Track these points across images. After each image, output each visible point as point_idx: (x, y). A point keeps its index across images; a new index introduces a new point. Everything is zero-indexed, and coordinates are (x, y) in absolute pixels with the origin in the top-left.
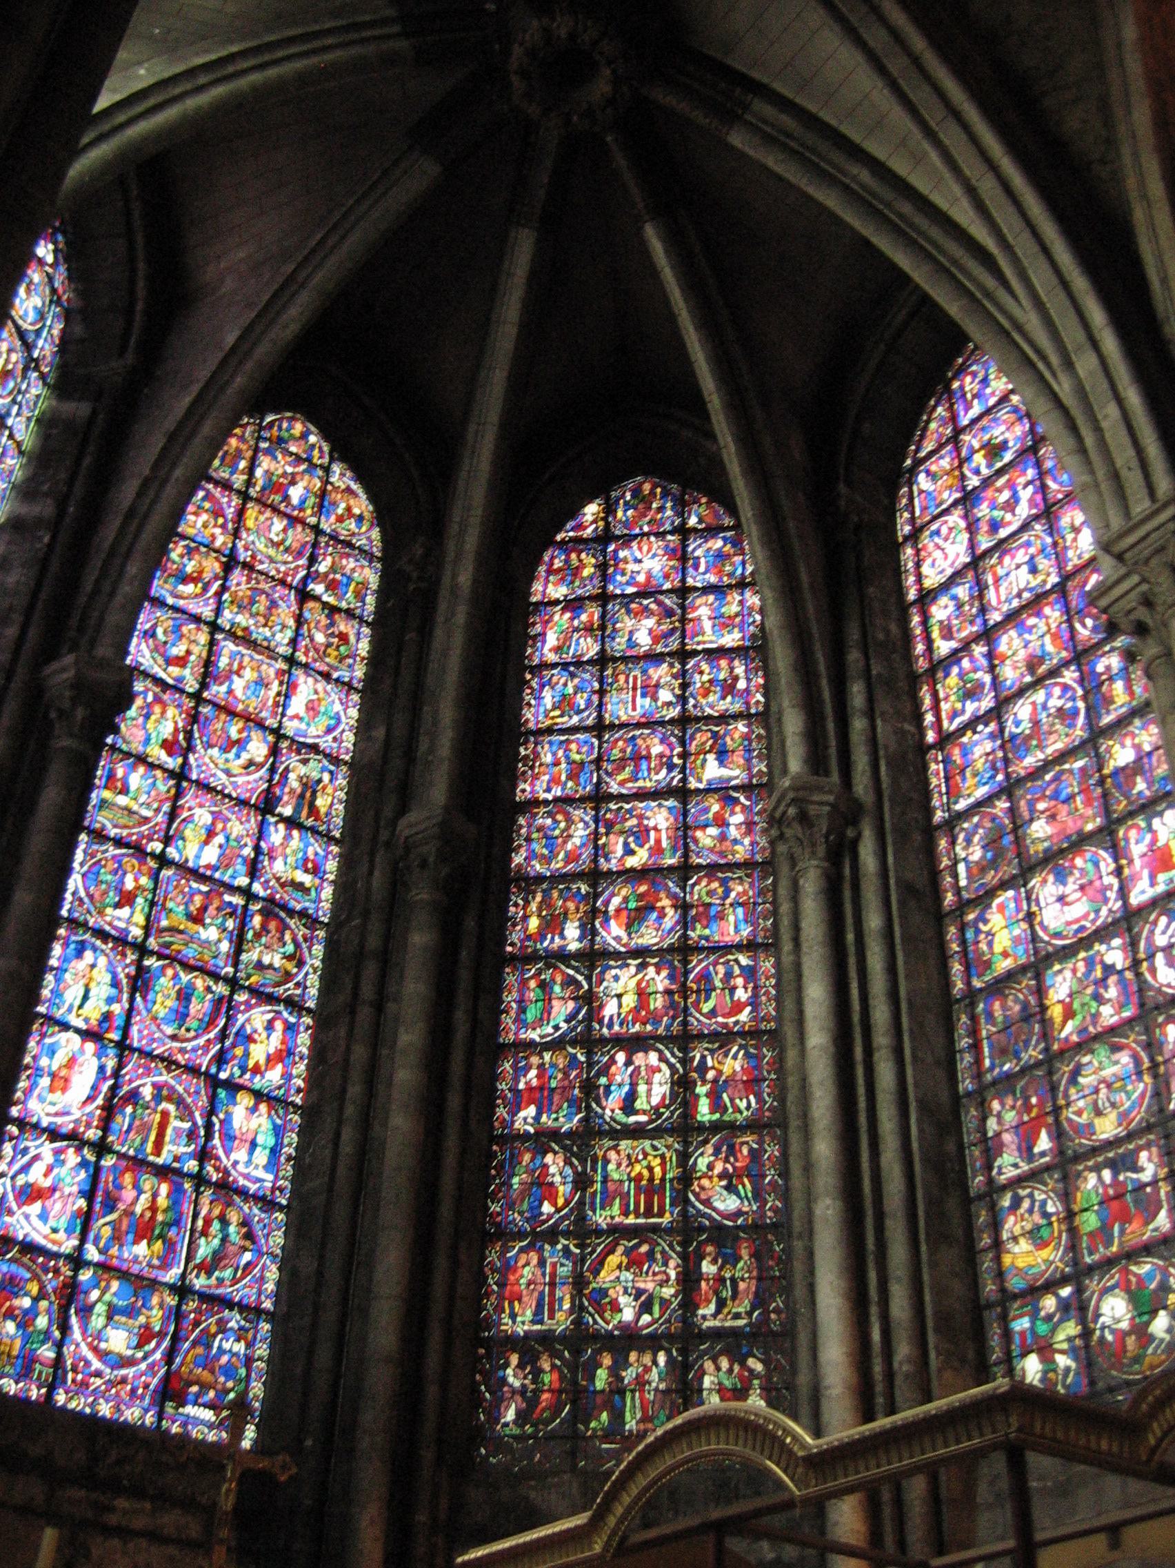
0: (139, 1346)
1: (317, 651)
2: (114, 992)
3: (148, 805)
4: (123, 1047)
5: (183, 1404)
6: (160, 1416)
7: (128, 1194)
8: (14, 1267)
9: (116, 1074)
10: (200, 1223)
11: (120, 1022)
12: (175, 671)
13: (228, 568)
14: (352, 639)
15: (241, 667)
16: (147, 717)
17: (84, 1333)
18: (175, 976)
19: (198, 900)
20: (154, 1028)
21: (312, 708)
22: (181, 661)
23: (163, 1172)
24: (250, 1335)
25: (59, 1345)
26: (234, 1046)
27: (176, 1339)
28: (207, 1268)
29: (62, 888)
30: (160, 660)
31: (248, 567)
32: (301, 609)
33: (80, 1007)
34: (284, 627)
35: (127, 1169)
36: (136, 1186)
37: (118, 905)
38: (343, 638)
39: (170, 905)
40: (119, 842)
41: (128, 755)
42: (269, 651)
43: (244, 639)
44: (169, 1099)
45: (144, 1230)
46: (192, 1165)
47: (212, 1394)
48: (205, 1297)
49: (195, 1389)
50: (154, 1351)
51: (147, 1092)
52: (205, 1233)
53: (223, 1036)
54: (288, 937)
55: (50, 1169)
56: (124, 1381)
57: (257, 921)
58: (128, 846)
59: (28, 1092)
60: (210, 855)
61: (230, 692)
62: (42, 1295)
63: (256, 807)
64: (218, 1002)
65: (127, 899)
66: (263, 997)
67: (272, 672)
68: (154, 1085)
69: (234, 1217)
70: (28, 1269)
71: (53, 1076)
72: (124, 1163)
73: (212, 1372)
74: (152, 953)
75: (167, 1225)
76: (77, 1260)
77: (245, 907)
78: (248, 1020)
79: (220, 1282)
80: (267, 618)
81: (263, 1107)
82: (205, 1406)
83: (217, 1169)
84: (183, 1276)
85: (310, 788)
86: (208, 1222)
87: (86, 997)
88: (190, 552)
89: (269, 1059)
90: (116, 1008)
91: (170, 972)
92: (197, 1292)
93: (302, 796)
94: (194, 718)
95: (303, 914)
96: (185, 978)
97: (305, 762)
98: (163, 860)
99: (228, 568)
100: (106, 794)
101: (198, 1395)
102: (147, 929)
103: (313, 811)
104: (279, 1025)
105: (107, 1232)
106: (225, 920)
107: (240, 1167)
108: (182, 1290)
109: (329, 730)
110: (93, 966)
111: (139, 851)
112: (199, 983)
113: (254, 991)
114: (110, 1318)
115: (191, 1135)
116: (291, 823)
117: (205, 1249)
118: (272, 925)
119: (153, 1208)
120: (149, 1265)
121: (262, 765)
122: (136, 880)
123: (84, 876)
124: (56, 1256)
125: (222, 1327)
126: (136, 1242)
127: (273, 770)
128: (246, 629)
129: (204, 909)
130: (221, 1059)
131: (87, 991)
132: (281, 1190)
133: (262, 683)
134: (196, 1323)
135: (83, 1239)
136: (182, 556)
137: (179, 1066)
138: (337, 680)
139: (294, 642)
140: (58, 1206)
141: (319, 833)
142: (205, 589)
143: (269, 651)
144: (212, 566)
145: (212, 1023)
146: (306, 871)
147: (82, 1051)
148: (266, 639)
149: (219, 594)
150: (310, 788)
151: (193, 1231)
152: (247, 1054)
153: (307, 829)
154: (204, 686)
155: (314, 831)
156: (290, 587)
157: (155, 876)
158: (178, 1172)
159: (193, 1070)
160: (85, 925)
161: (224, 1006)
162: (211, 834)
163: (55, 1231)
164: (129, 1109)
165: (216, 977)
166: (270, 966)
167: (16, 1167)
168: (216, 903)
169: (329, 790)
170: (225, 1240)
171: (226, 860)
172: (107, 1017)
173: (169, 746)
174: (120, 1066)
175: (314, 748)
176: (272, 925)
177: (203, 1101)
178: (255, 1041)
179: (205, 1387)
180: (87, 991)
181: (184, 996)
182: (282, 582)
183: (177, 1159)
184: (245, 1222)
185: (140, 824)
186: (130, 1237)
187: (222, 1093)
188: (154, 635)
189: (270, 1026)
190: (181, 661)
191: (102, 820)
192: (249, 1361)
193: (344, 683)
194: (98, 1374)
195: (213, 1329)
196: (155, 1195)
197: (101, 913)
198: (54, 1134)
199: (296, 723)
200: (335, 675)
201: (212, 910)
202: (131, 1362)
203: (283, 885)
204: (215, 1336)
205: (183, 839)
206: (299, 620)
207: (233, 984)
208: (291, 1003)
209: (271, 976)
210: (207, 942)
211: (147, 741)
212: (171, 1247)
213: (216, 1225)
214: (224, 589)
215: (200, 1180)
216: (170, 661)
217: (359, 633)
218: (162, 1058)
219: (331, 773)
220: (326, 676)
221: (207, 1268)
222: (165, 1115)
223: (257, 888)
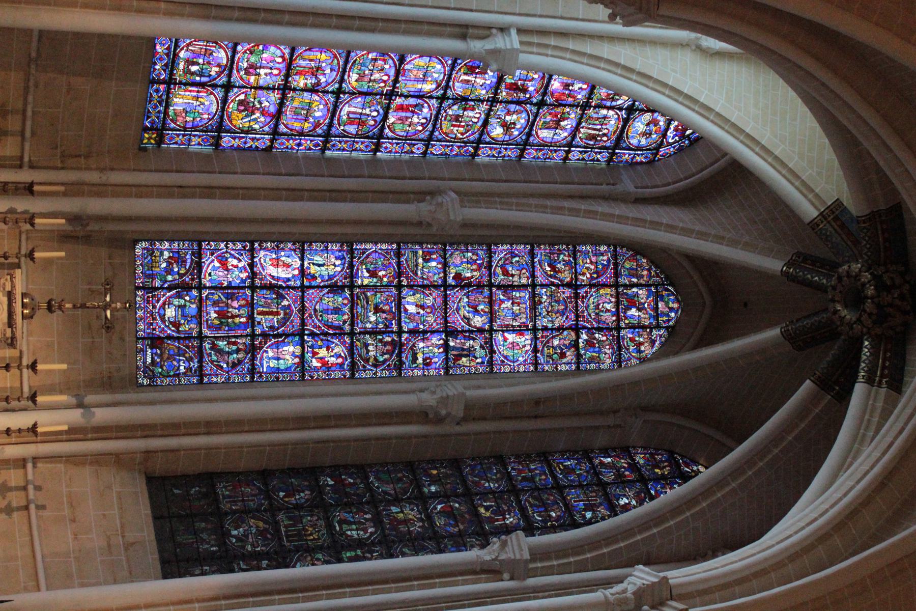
0: (170, 322)
1: (548, 342)
2: (326, 278)
3: (423, 273)
4: (303, 288)
5: (152, 348)
6: (143, 339)
7: (235, 304)
8: (189, 261)
9: (288, 287)
10: (233, 340)
11: (313, 283)
12: (499, 270)
13: (569, 285)
14: (565, 360)
15: (519, 304)
16: (468, 262)
17: (170, 297)
18: (346, 305)
19: (386, 308)
20: (316, 300)
21: (513, 345)
22: (506, 273)
23: (251, 317)
24: (189, 373)
25: (162, 288)
26: (322, 340)
27: (178, 339)
28: (214, 347)
29: (366, 242)
30: (501, 262)
31: (577, 296)
32: (567, 329)
33: (314, 264)
34: (552, 322)
35: (247, 301)
36: (241, 307)
37: (368, 271)
38: (563, 355)
39: (379, 296)
40: (399, 264)
41: (445, 258)
42: (534, 318)
43: (535, 303)
44: (285, 314)
45: (222, 315)
46: (258, 331)
47: (158, 360)
48: (200, 348)
49: (159, 352)
50: (170, 329)
51: (285, 303)
52: (229, 343)
53: (326, 334)
54: (386, 356)
55: (236, 267)
56: (154, 319)
57: (388, 339)
58: (399, 268)
59: (266, 249)
60: (412, 309)
61: (502, 301)
62: (181, 276)
63: (446, 327)
64: (340, 328)
65: (373, 274)
66: (351, 349)
67: (524, 320)
68: (289, 305)
69: (241, 356)
70: (190, 267)
71: (278, 259)
72: (249, 299)
73: (168, 358)
74: (352, 291)
75: (228, 325)
76: (200, 288)
77: (392, 332)
78: (337, 344)
79: (209, 355)
80: (552, 311)
81: (297, 360)
82: (152, 358)
83: (260, 343)
84: (207, 337)
85: (470, 353)
86: (235, 343)
87: (319, 265)
88: (567, 263)
89: (322, 359)
90: (319, 280)
91: (346, 302)
92: (201, 345)
93: (463, 350)
94: (480, 286)
95: (401, 363)
96: (346, 309)
97: (482, 347)
98: (399, 287)
99: (569, 285)
100: (420, 252)
101: (156, 354)
102: (362, 286)
103: (458, 357)
104: (340, 360)
105: (216, 297)
106: (383, 323)
107: (265, 355)
108: (201, 337)
109: (506, 357)
110: (334, 265)
111: (399, 275)
112: (346, 317)
113: (352, 343)
114: (179, 306)
115: (272, 328)
116: (446, 346)
117: (222, 344)
118: (389, 347)
119: (233, 317)
120: (207, 320)
121: (470, 325)
122: (384, 276)
123: (375, 251)
124: (200, 279)
125: (190, 359)
126: (215, 312)
127: (471, 332)
128: (541, 303)
129: (384, 312)
130: (312, 334)
131: (323, 265)
132: (261, 376)
133: (515, 316)
134: (188, 347)
135: (209, 288)
136: (564, 261)
137: (303, 315)
138: (536, 357)
139: (545, 329)
140: (221, 274)
141: (447, 363)
142: (551, 276)
143: (534, 318)
144: (567, 276)
145: (329, 327)
146: (424, 360)
147: (294, 269)
148: (540, 314)
149: (553, 284)
150: (470, 353)
151: (229, 337)
152: (320, 347)
153: (447, 355)
154: (499, 287)
155: (447, 359)
156: (577, 320)
157: (388, 285)
158: (253, 326)
159: (303, 324)
160: (352, 258)
161: (339, 332)
162: (422, 307)
163: (210, 275)
164: (274, 296)
165: (352, 324)
166: (368, 351)
167: (233, 252)
168: (389, 317)
169: (473, 364)
170: (229, 353)
171: (411, 317)
172: (314, 278)
173: (458, 276)
174: (294, 288)
175: (492, 352)
176: (389, 347)
177: (290, 330)
178: (328, 350)
179: (161, 356)
180: (323, 265)
181: (337, 311)
182: (577, 316)
183: (259, 323)
184: (240, 362)
185: (412, 272)
186: (217, 309)
187: (297, 338)
188: (513, 257)
189: (338, 356)
190: (506, 273)
191: (407, 254)
192: (177, 375)
193: (536, 361)
194: (154, 307)
195: (187, 355)
196: (239, 316)
197: (361, 263)
198: (252, 265)
199: (501, 339)
200: (539, 355)
201: (384, 315)
202: (163, 321)
203: (411, 348)
204: (184, 356)
205: (414, 294)
206: (561, 329)
207: (352, 334)
208: (353, 365)
209: (364, 351)
210: (368, 317)
211: (456, 266)
212: (218, 328)
213: (235, 348)
214: (558, 286)
215: (253, 336)
216: (502, 267)
217: (570, 363)
218: (303, 306)
219: (483, 363)
220: (535, 350)
221: (214, 347)
222: (278, 313)
223: (405, 336)
